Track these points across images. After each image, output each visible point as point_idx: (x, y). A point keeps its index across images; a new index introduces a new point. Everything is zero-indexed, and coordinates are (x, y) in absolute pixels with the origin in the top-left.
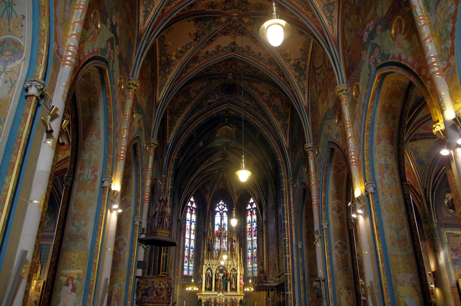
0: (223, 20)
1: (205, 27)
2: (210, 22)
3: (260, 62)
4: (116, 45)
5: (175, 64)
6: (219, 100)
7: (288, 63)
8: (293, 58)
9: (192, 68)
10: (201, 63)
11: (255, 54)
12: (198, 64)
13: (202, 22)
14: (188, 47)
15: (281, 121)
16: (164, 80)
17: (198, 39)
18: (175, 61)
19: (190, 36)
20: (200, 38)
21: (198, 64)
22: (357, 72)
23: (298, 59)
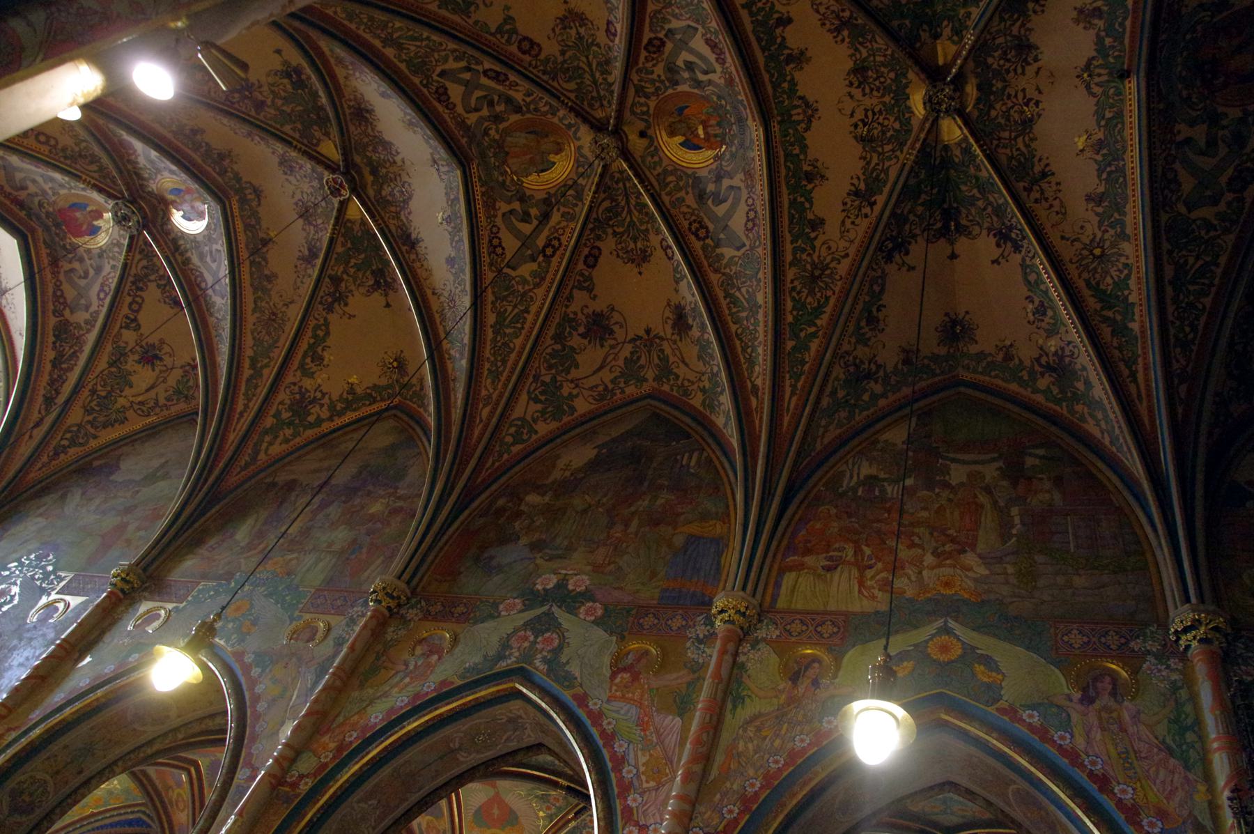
1: (980, 203)
4: (573, 611)
5: (1071, 347)
9: (1128, 276)
13: (964, 211)
14: (1032, 277)
16: (1100, 416)
17: (1013, 236)
20: (1010, 228)
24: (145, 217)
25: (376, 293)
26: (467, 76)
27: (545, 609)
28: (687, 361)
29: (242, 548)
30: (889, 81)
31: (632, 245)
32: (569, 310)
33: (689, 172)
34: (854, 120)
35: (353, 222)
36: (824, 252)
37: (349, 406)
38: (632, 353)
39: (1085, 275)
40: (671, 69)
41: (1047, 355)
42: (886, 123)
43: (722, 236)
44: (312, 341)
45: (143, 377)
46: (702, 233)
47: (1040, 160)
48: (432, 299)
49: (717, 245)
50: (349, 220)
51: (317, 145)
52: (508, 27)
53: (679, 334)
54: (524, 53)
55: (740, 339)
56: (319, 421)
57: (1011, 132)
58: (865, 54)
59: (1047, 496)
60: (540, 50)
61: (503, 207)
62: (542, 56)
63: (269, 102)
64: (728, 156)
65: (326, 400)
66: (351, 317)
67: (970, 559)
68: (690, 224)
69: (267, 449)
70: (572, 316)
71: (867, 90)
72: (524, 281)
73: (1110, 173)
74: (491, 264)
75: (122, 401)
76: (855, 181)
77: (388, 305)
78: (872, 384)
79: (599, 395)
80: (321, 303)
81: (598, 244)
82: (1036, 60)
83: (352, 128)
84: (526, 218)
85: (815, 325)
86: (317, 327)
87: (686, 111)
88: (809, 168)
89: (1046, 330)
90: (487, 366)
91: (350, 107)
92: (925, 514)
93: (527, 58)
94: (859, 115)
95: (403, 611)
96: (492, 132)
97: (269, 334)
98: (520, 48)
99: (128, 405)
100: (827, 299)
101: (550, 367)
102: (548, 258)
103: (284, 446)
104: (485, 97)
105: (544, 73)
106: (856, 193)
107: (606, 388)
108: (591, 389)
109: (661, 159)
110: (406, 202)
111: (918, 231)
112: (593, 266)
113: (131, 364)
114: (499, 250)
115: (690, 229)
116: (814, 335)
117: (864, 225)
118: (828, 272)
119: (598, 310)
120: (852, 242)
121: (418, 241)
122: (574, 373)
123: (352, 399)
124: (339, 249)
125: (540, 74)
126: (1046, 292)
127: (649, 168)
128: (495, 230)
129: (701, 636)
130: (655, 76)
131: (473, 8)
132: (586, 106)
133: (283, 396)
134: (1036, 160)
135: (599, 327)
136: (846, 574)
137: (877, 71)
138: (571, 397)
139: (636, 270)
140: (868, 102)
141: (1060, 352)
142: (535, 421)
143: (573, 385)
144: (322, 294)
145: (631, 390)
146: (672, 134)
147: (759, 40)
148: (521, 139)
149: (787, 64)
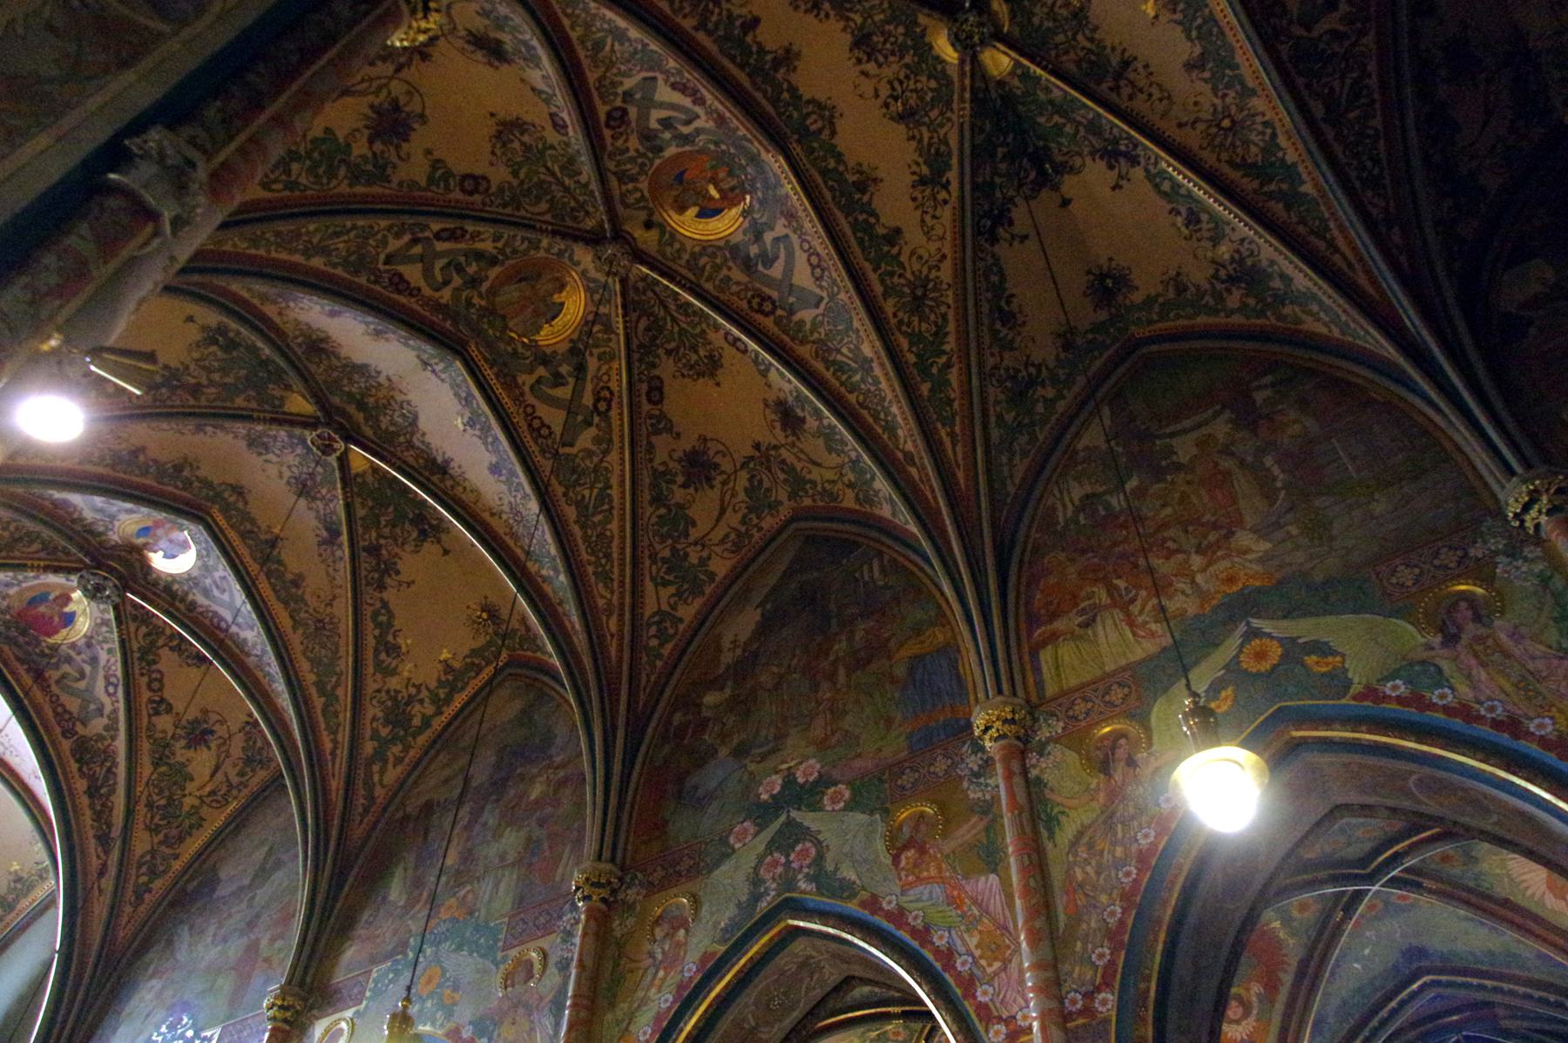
1: (1069, 129)
2: (1041, 114)
4: (815, 807)
5: (1246, 245)
9: (1274, 136)
14: (1166, 186)
16: (1315, 308)
17: (1123, 148)
18: (1235, 246)
19: (1124, 183)
20: (1116, 142)
24: (120, 577)
25: (426, 545)
26: (417, 249)
27: (783, 818)
28: (814, 458)
29: (404, 907)
30: (901, 39)
31: (694, 357)
32: (656, 464)
33: (722, 243)
34: (880, 101)
35: (363, 475)
36: (916, 267)
37: (453, 689)
38: (750, 480)
39: (1224, 156)
40: (648, 136)
41: (1224, 267)
42: (919, 86)
43: (791, 300)
44: (377, 632)
45: (201, 762)
46: (767, 307)
47: (1113, 49)
48: (493, 522)
49: (791, 312)
50: (357, 475)
51: (282, 406)
52: (440, 172)
53: (794, 434)
54: (471, 193)
55: (867, 408)
56: (427, 723)
57: (1065, 32)
58: (859, 20)
59: (1297, 427)
60: (488, 181)
61: (526, 380)
62: (493, 189)
63: (204, 381)
64: (757, 206)
65: (424, 694)
66: (409, 584)
67: (1243, 539)
68: (749, 302)
69: (381, 780)
70: (661, 468)
71: (881, 59)
72: (589, 454)
73: (1199, 28)
74: (543, 452)
75: (189, 802)
76: (914, 168)
77: (446, 552)
78: (1040, 391)
79: (734, 543)
80: (368, 584)
81: (656, 372)
83: (313, 368)
84: (558, 380)
85: (944, 352)
86: (376, 614)
87: (687, 176)
88: (855, 178)
89: (1210, 239)
90: (590, 569)
92: (1169, 511)
93: (477, 198)
94: (885, 91)
95: (621, 896)
96: (476, 300)
97: (323, 646)
98: (463, 191)
99: (197, 802)
100: (944, 316)
101: (663, 538)
102: (605, 415)
103: (399, 769)
104: (449, 264)
105: (505, 206)
106: (922, 181)
107: (739, 534)
108: (722, 542)
109: (682, 244)
110: (414, 422)
111: (1011, 193)
112: (661, 401)
113: (180, 753)
114: (544, 432)
115: (751, 307)
116: (948, 365)
117: (946, 214)
118: (931, 285)
119: (688, 448)
120: (942, 238)
121: (447, 462)
122: (694, 534)
123: (453, 678)
124: (361, 512)
125: (500, 210)
126: (1189, 195)
127: (673, 260)
128: (529, 410)
129: (976, 768)
130: (632, 153)
131: (389, 171)
132: (569, 223)
133: (373, 710)
134: (1108, 50)
135: (699, 467)
136: (1109, 622)
137: (883, 33)
138: (703, 562)
139: (711, 383)
140: (888, 72)
141: (1237, 256)
142: (674, 608)
143: (699, 548)
144: (364, 573)
145: (769, 523)
146: (682, 209)
147: (732, 59)
148: (511, 293)
149: (776, 71)
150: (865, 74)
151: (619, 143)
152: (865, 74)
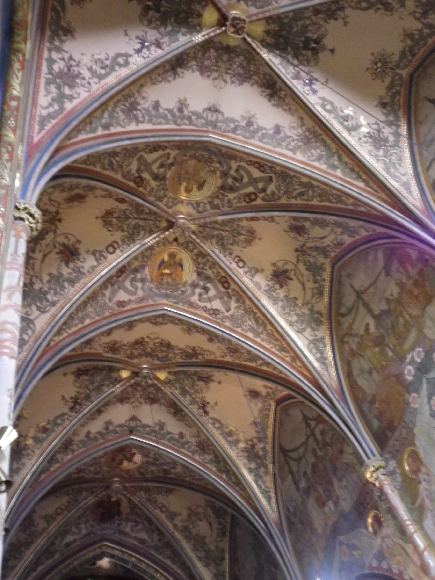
0: (125, 374)
1: (91, 387)
3: (182, 450)
6: (85, 536)
7: (234, 448)
8: (242, 438)
10: (76, 453)
11: (172, 435)
12: (70, 456)
14: (59, 421)
15: (211, 568)
21: (70, 456)
22: (404, 431)
23: (251, 440)
26: (260, 185)
28: (47, 259)
40: (208, 279)
50: (207, 5)
61: (173, 153)
63: (314, 18)
82: (146, 403)
84: (162, 166)
91: (281, 89)
96: (218, 165)
121: (175, 74)
126: (53, 431)
130: (207, 268)
139: (99, 214)
150: (157, 338)
151: (215, 271)
152: (157, 338)
